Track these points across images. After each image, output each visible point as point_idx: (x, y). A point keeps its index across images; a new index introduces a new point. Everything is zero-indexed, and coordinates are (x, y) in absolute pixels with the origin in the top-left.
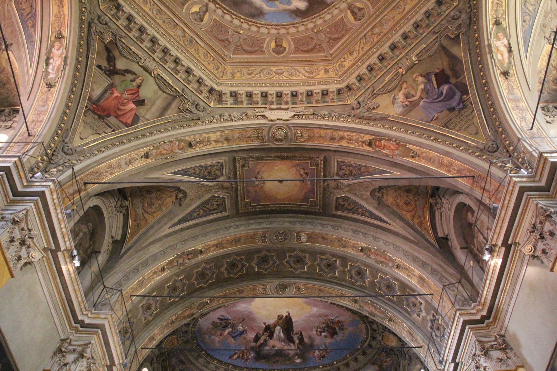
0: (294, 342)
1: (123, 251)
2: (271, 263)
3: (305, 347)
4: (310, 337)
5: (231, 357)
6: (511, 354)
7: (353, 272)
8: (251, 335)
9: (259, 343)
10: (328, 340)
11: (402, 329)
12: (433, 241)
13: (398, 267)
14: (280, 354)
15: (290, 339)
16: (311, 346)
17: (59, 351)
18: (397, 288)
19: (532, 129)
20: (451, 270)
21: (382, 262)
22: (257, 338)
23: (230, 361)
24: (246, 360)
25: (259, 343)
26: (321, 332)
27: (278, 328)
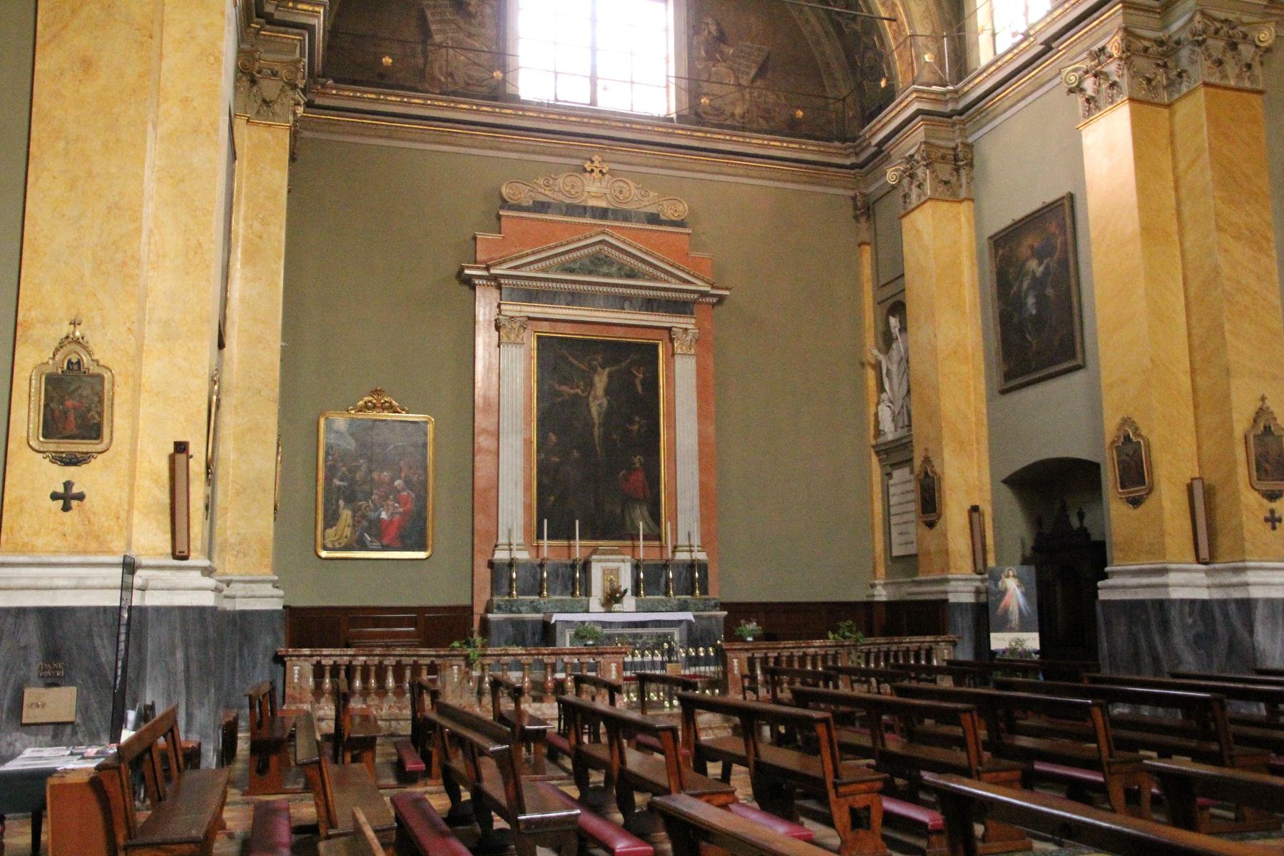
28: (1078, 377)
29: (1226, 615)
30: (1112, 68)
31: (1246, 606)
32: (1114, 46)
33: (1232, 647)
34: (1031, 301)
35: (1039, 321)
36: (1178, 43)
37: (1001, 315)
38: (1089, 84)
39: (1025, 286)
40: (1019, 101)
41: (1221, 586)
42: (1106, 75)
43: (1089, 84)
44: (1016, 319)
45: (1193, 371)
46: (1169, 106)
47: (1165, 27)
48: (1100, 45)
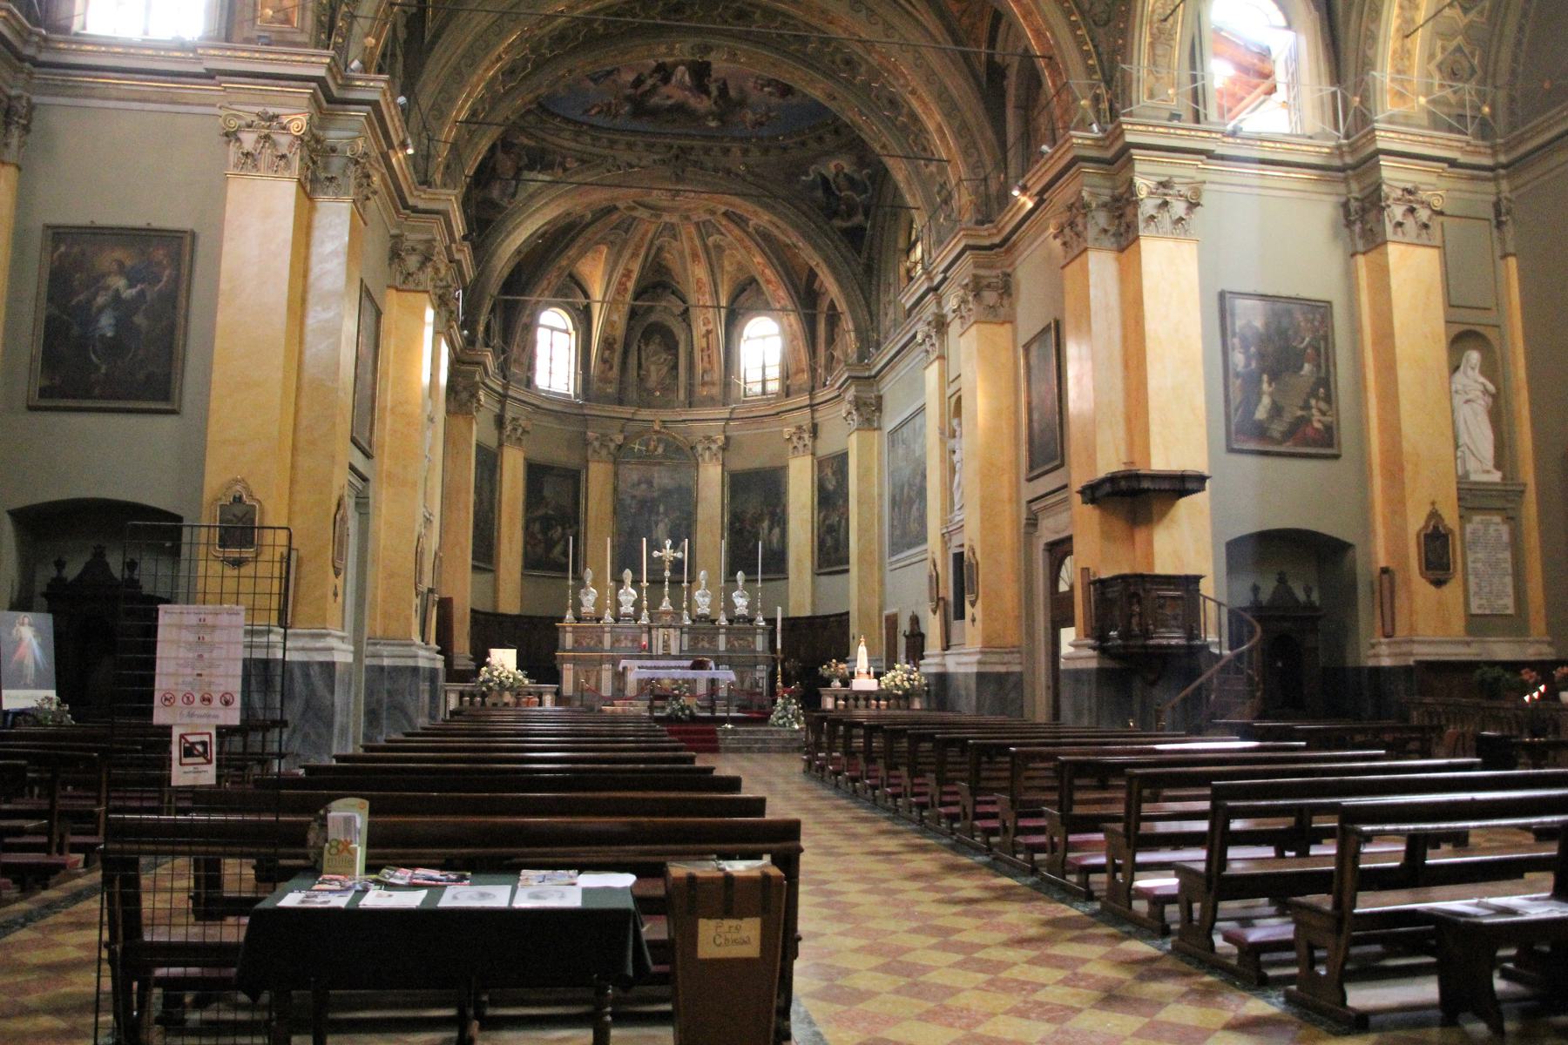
0: (708, 93)
1: (428, 38)
2: (688, 12)
3: (728, 105)
4: (741, 90)
5: (586, 111)
6: (1005, 302)
7: (838, 58)
8: (630, 77)
9: (640, 91)
10: (775, 100)
11: (899, 172)
12: (982, 70)
13: (913, 92)
14: (680, 109)
15: (700, 87)
16: (742, 103)
17: (395, 255)
18: (905, 111)
19: (1165, 20)
20: (990, 134)
21: (888, 71)
22: (638, 82)
23: (585, 118)
24: (615, 117)
25: (640, 91)
26: (763, 86)
27: (682, 68)
28: (167, 422)
29: (307, 676)
30: (284, 140)
31: (329, 667)
32: (298, 122)
33: (307, 702)
34: (106, 324)
35: (114, 347)
36: (333, 150)
37: (49, 321)
38: (249, 140)
39: (100, 300)
40: (134, 100)
41: (303, 649)
42: (275, 145)
43: (249, 140)
44: (76, 330)
45: (294, 448)
46: (311, 199)
47: (322, 128)
48: (277, 111)
